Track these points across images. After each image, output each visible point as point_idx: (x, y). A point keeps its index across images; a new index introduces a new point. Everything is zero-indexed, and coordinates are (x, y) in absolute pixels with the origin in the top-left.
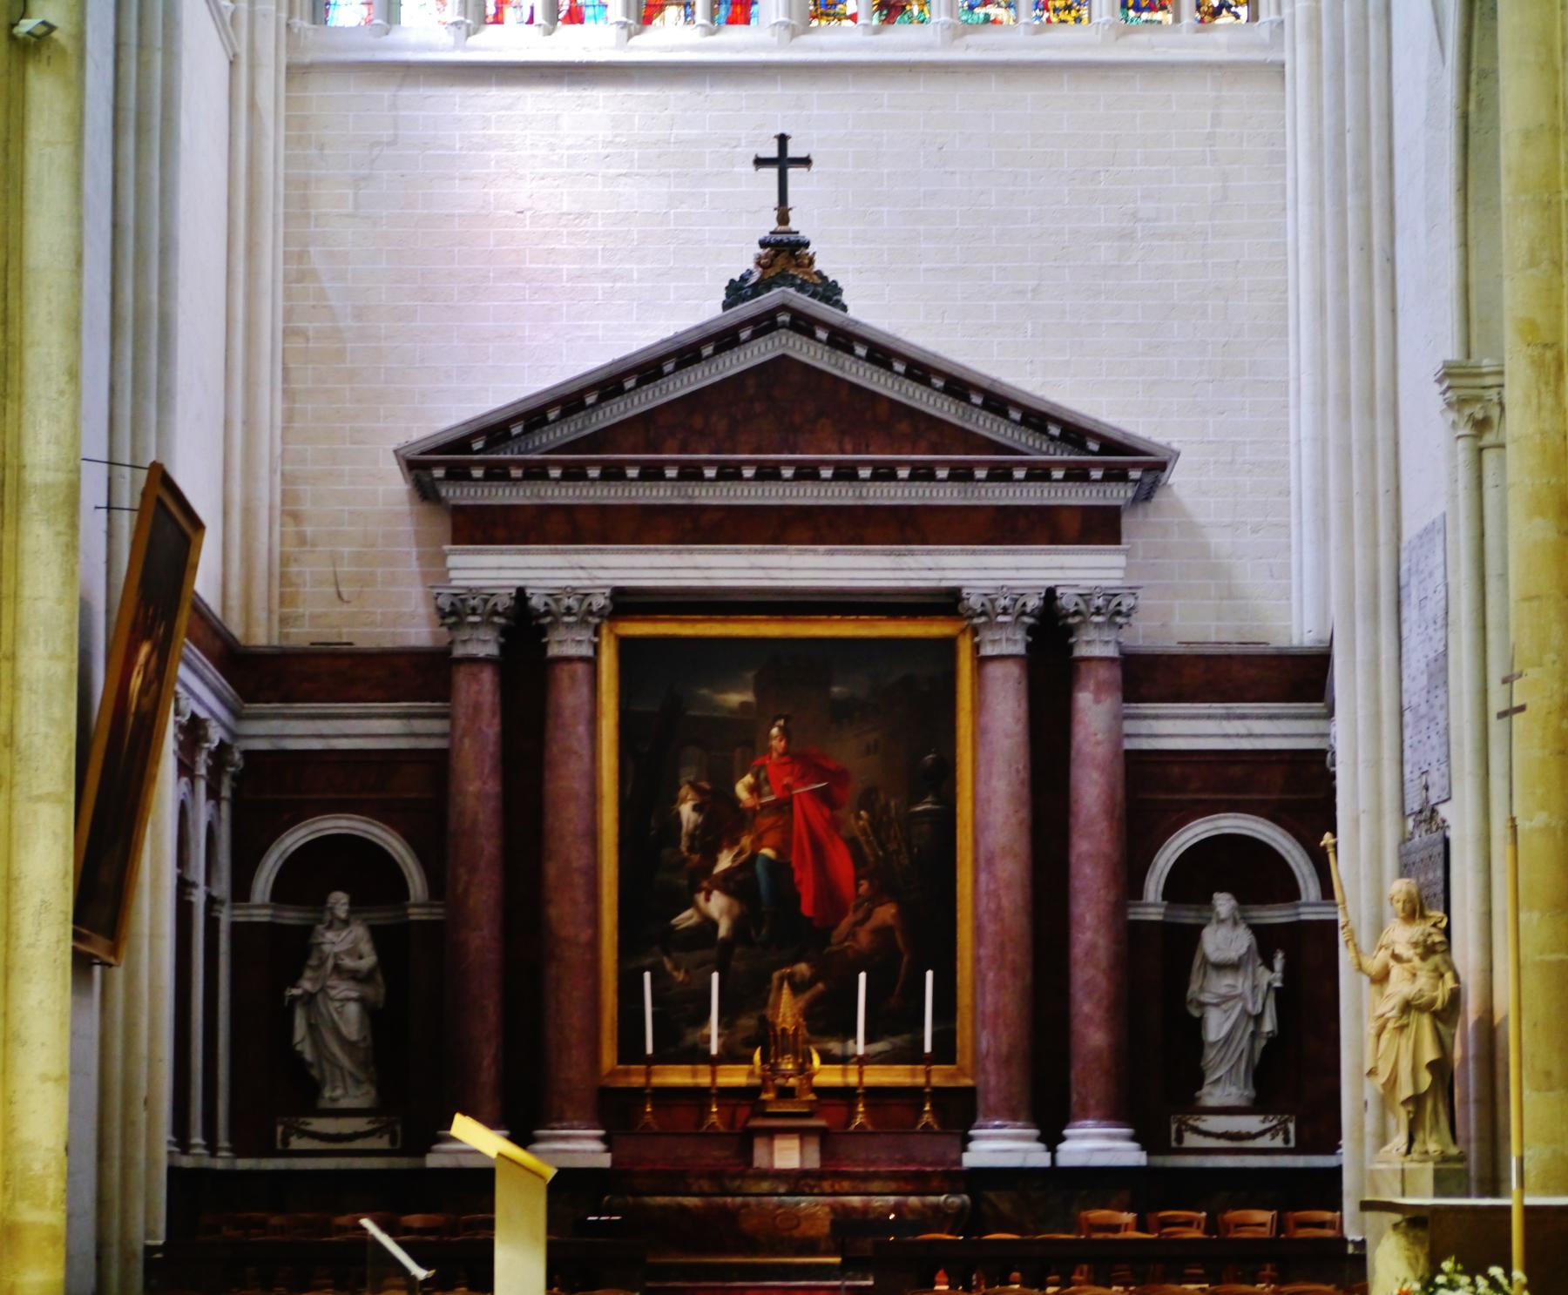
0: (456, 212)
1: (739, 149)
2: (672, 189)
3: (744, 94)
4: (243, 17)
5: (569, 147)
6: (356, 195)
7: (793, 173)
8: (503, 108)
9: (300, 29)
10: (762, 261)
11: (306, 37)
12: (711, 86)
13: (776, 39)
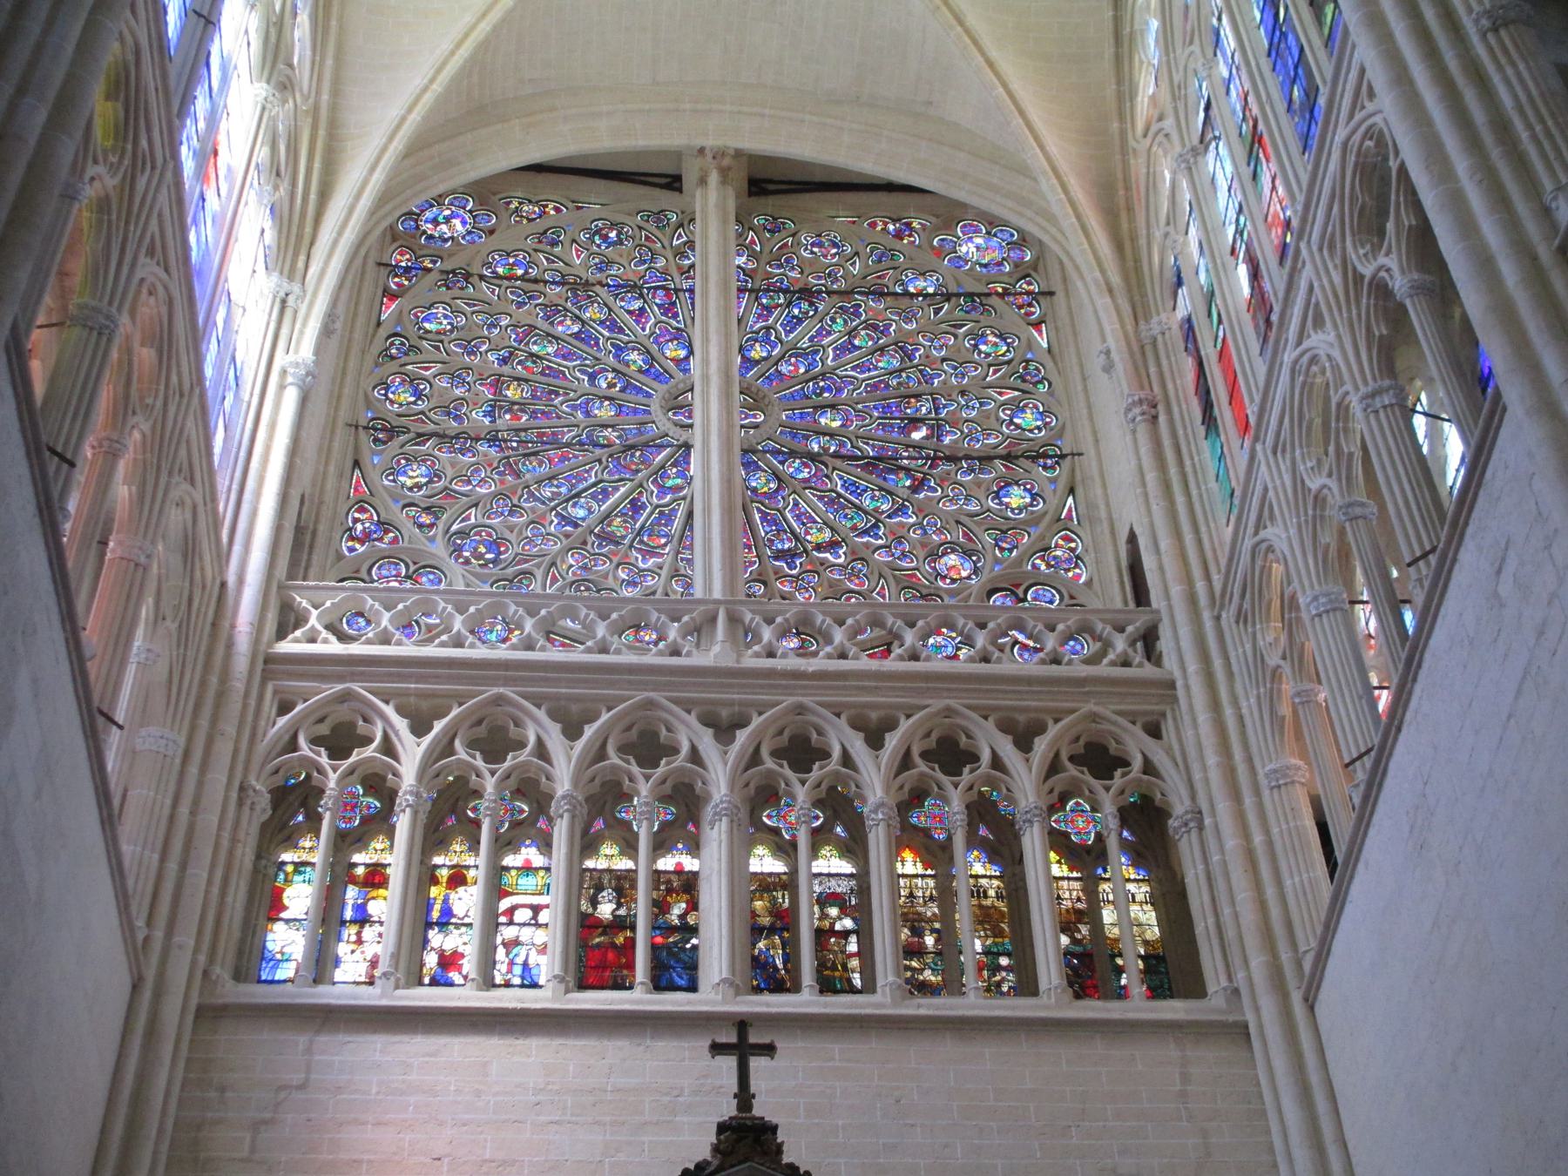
0: (366, 1157)
1: (680, 1099)
2: (608, 1137)
3: (686, 1045)
4: (157, 945)
5: (497, 1094)
6: (253, 1141)
7: (757, 1063)
8: (431, 1055)
9: (218, 976)
10: (722, 1147)
11: (223, 986)
12: (652, 1038)
13: (720, 997)
